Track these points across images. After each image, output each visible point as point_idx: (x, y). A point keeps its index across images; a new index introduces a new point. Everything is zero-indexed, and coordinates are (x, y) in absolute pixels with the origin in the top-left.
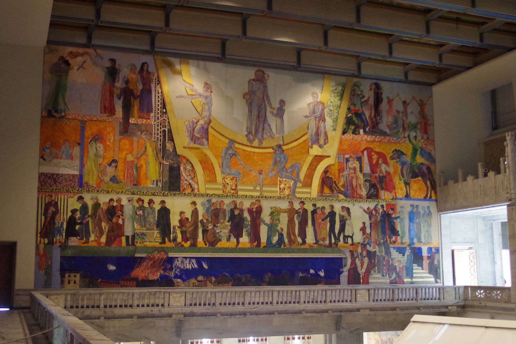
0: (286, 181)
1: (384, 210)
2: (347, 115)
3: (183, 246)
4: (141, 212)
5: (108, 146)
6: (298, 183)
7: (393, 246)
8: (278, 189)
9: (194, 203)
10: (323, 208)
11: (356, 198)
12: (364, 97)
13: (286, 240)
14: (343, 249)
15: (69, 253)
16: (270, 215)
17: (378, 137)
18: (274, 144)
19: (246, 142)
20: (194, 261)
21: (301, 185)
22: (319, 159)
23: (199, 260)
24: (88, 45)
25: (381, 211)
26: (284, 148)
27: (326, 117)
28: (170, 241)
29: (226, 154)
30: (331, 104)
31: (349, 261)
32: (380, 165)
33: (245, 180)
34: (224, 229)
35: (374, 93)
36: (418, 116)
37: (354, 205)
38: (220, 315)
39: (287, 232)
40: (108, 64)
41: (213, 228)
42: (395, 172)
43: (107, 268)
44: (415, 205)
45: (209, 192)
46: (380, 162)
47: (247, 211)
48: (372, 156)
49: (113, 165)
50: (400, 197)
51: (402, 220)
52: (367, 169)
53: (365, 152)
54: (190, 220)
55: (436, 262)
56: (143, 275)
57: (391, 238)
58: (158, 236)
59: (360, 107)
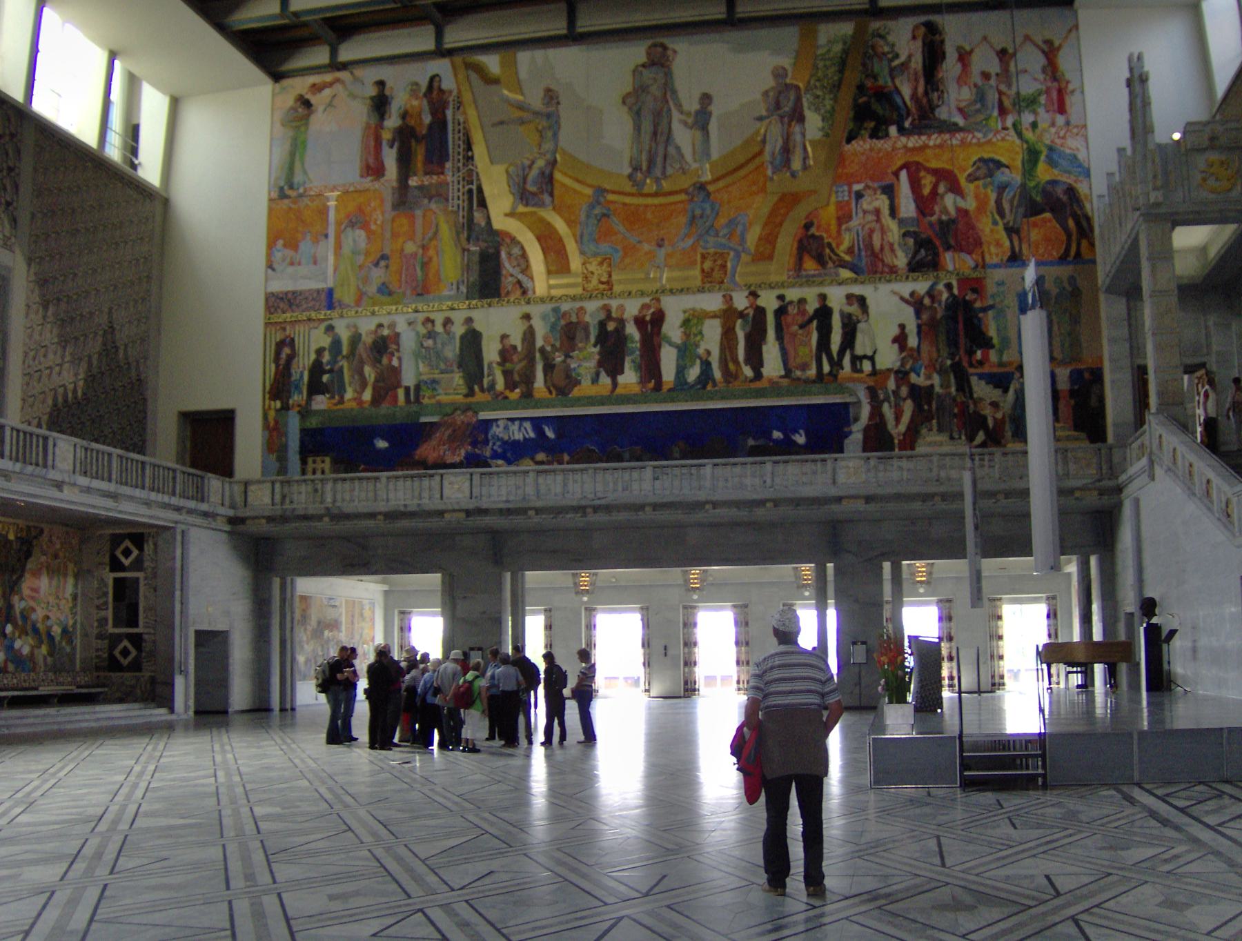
0: (716, 253)
1: (952, 294)
2: (855, 100)
3: (506, 398)
5: (373, 233)
7: (979, 370)
9: (527, 317)
10: (802, 301)
11: (882, 273)
12: (897, 56)
13: (717, 374)
14: (850, 385)
15: (313, 423)
17: (935, 136)
18: (685, 182)
19: (628, 187)
20: (528, 425)
21: (749, 258)
22: (790, 200)
23: (537, 423)
25: (945, 296)
26: (711, 188)
28: (482, 390)
29: (588, 217)
30: (818, 84)
32: (942, 197)
33: (628, 260)
35: (924, 44)
36: (1041, 77)
37: (876, 289)
39: (720, 358)
40: (372, 91)
41: (564, 361)
42: (982, 207)
43: (374, 445)
45: (554, 292)
46: (942, 189)
48: (919, 180)
49: (383, 263)
50: (995, 260)
52: (907, 207)
53: (903, 175)
54: (519, 349)
55: (1094, 402)
56: (435, 455)
57: (971, 353)
58: (461, 382)
59: (889, 80)
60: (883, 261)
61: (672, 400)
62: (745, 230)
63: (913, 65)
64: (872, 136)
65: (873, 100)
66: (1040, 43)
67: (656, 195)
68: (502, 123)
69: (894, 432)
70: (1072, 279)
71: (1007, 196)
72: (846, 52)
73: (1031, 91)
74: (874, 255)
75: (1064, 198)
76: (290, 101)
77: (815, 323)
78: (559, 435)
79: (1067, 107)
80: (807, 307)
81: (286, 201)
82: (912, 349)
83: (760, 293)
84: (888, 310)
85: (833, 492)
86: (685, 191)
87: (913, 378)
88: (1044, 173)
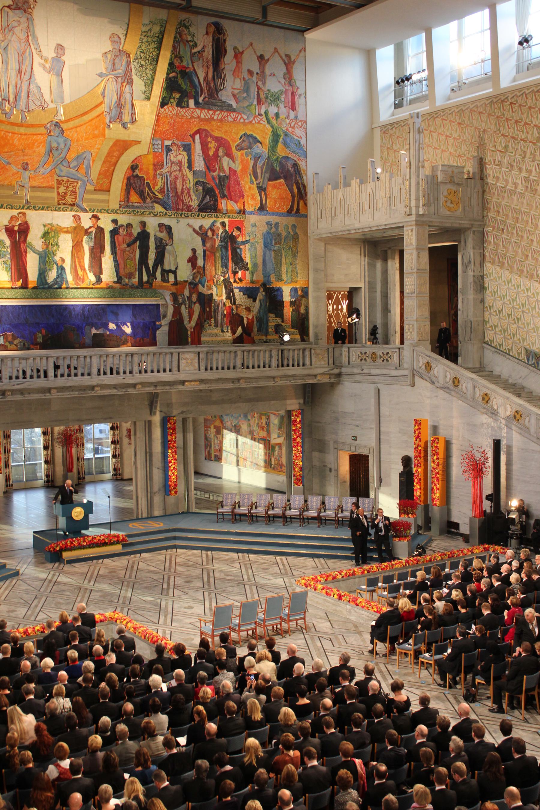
0: (68, 181)
2: (168, 74)
6: (88, 185)
8: (55, 195)
10: (129, 226)
11: (182, 210)
12: (196, 45)
14: (161, 291)
16: (42, 238)
17: (218, 112)
25: (221, 231)
26: (64, 126)
27: (135, 77)
30: (142, 55)
31: (171, 310)
35: (213, 39)
36: (283, 81)
39: (72, 265)
46: (220, 154)
47: (4, 231)
50: (251, 209)
51: (253, 245)
52: (199, 164)
53: (197, 137)
55: (302, 311)
57: (235, 273)
60: (183, 202)
62: (89, 166)
63: (206, 53)
65: (179, 76)
66: (284, 57)
67: (21, 125)
69: (188, 326)
73: (276, 91)
74: (177, 195)
75: (292, 170)
77: (138, 242)
80: (133, 231)
82: (200, 267)
83: (100, 215)
85: (182, 377)
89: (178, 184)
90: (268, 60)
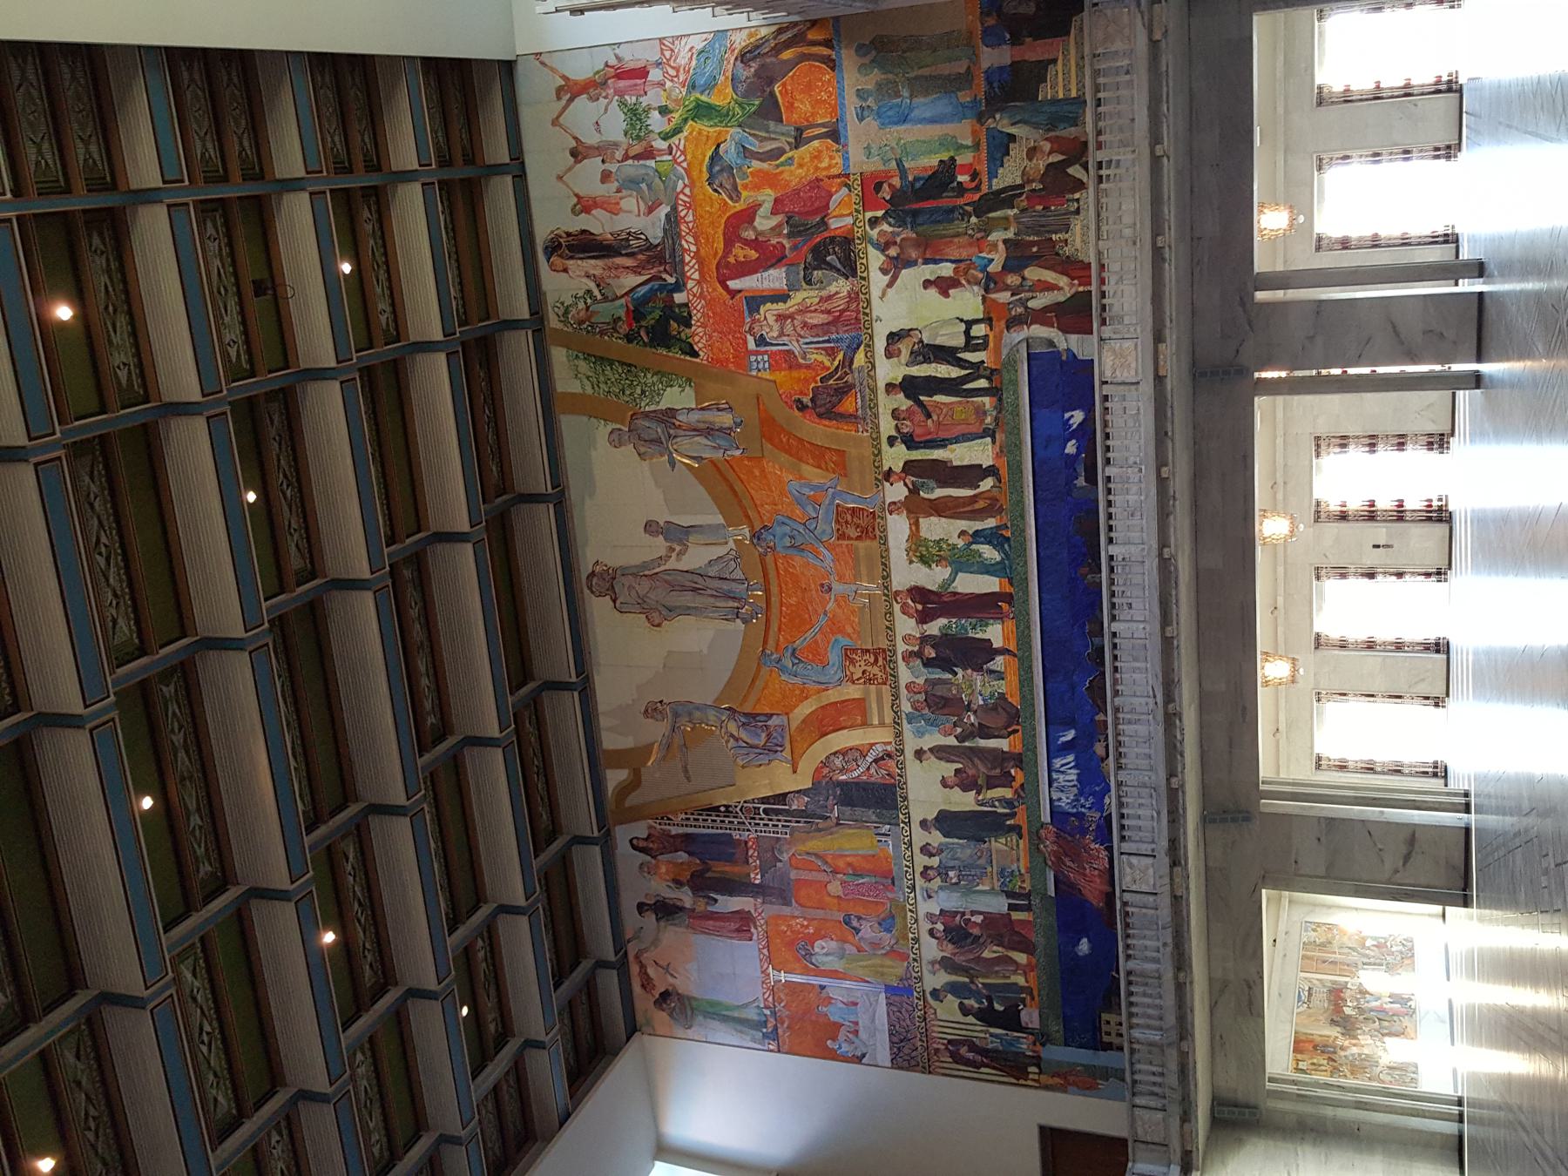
0: (837, 522)
1: (884, 217)
2: (645, 345)
4: (951, 874)
5: (817, 930)
7: (985, 179)
8: (861, 545)
9: (919, 754)
10: (895, 414)
11: (858, 312)
12: (589, 292)
13: (991, 523)
14: (1005, 352)
15: (1056, 1028)
20: (1058, 763)
22: (770, 430)
23: (1054, 751)
24: (622, 966)
25: (885, 227)
26: (758, 526)
27: (663, 406)
28: (1013, 815)
31: (1038, 331)
32: (759, 234)
33: (850, 630)
34: (976, 686)
35: (572, 258)
37: (879, 319)
38: (1174, 780)
41: (975, 712)
44: (859, 103)
46: (749, 234)
49: (855, 923)
50: (838, 160)
52: (774, 279)
53: (732, 284)
58: (1003, 840)
59: (618, 303)
60: (842, 312)
61: (1026, 580)
63: (598, 272)
64: (689, 326)
66: (563, 102)
67: (767, 591)
68: (686, 771)
70: (861, 50)
71: (754, 145)
72: (588, 357)
75: (755, 65)
76: (661, 1017)
78: (1069, 724)
79: (640, 65)
81: (780, 1031)
83: (886, 468)
84: (909, 302)
85: (1147, 387)
86: (762, 557)
87: (994, 268)
88: (723, 97)
89: (815, 322)
90: (575, 138)
